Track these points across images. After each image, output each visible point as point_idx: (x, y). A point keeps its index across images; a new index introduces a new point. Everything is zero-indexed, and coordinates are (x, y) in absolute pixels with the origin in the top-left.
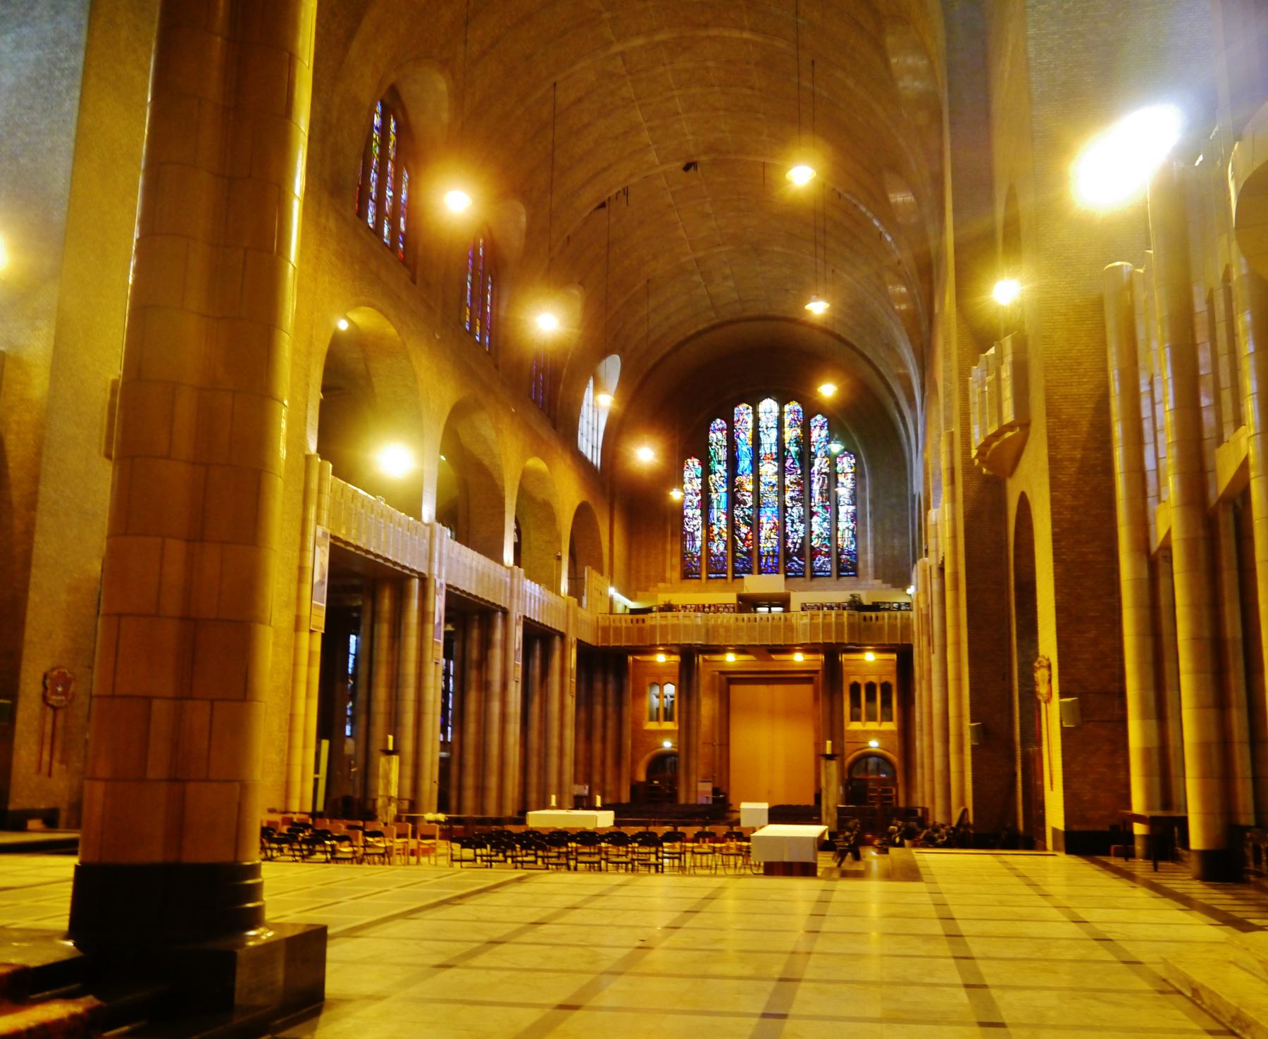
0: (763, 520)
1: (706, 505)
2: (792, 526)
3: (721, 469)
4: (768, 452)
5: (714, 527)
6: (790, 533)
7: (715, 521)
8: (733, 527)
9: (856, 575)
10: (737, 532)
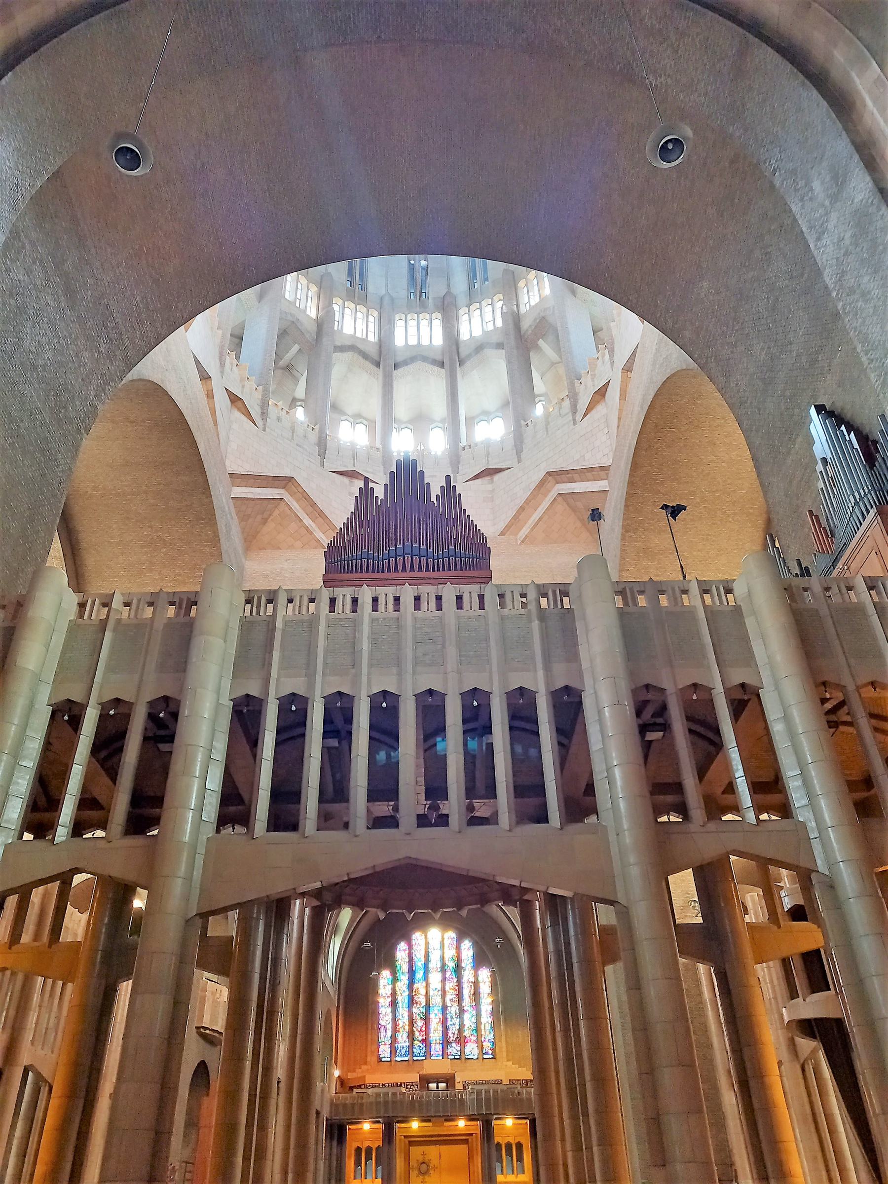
0: (432, 1016)
1: (394, 1004)
2: (451, 1021)
3: (404, 979)
4: (435, 966)
5: (400, 1021)
6: (450, 1026)
7: (400, 1017)
8: (412, 1022)
9: (494, 1058)
10: (415, 1026)
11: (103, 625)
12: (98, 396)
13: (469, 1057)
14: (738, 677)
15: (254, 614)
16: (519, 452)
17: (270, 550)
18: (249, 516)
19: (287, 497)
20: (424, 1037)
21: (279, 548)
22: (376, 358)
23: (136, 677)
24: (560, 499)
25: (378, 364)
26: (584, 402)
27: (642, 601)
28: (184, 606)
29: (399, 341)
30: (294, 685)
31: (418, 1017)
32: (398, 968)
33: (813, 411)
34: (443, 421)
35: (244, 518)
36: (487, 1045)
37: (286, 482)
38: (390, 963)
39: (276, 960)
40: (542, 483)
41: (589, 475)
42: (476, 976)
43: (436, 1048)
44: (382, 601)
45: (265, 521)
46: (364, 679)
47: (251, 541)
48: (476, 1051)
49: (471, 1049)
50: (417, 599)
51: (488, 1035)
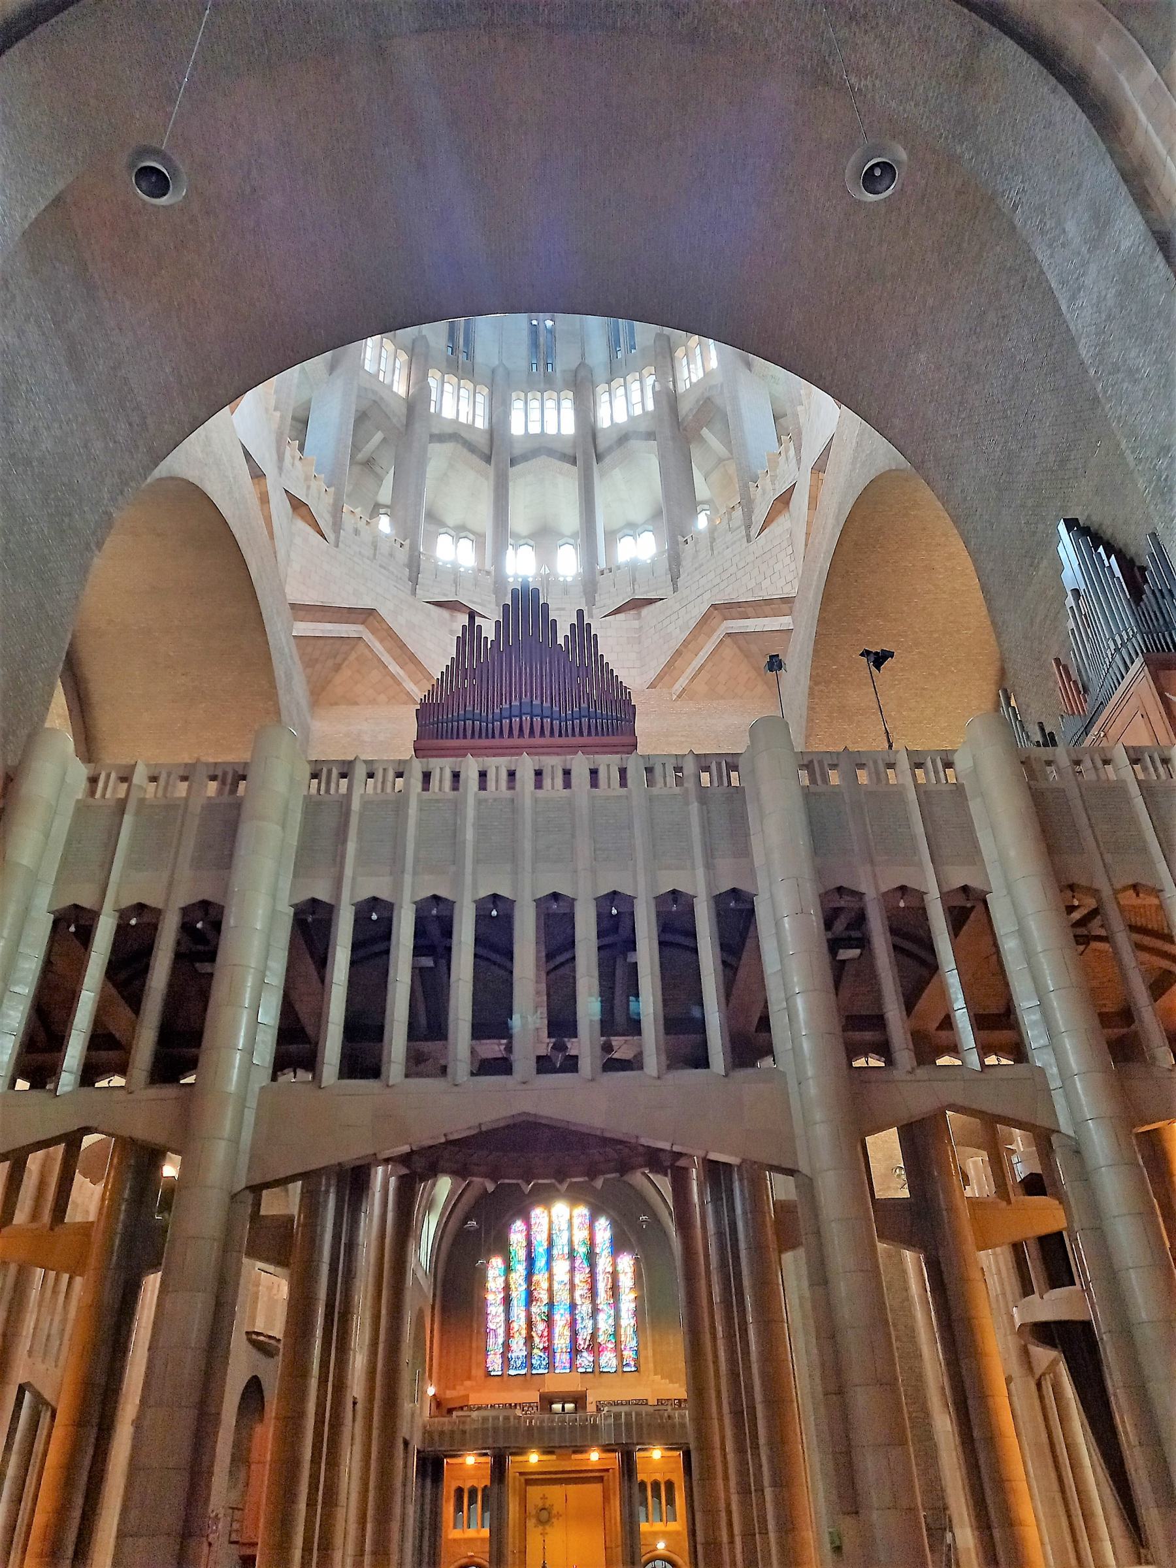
0: (557, 1317)
1: (507, 1301)
3: (520, 1269)
7: (515, 1319)
8: (530, 1324)
11: (121, 807)
12: (113, 499)
13: (605, 1370)
14: (959, 877)
15: (322, 792)
16: (674, 580)
17: (344, 707)
18: (317, 660)
19: (368, 636)
20: (546, 1345)
21: (356, 703)
22: (487, 451)
23: (165, 875)
24: (728, 641)
25: (488, 459)
26: (760, 513)
27: (834, 778)
28: (229, 780)
29: (517, 428)
30: (376, 886)
31: (538, 1319)
32: (513, 1254)
33: (1062, 527)
34: (574, 536)
35: (309, 663)
36: (628, 1354)
37: (366, 615)
38: (502, 1247)
39: (351, 1246)
40: (705, 619)
41: (767, 609)
42: (614, 1265)
43: (562, 1358)
44: (491, 776)
45: (337, 668)
46: (468, 879)
47: (319, 694)
48: (614, 1362)
49: (608, 1360)
50: (538, 773)
51: (629, 1341)
